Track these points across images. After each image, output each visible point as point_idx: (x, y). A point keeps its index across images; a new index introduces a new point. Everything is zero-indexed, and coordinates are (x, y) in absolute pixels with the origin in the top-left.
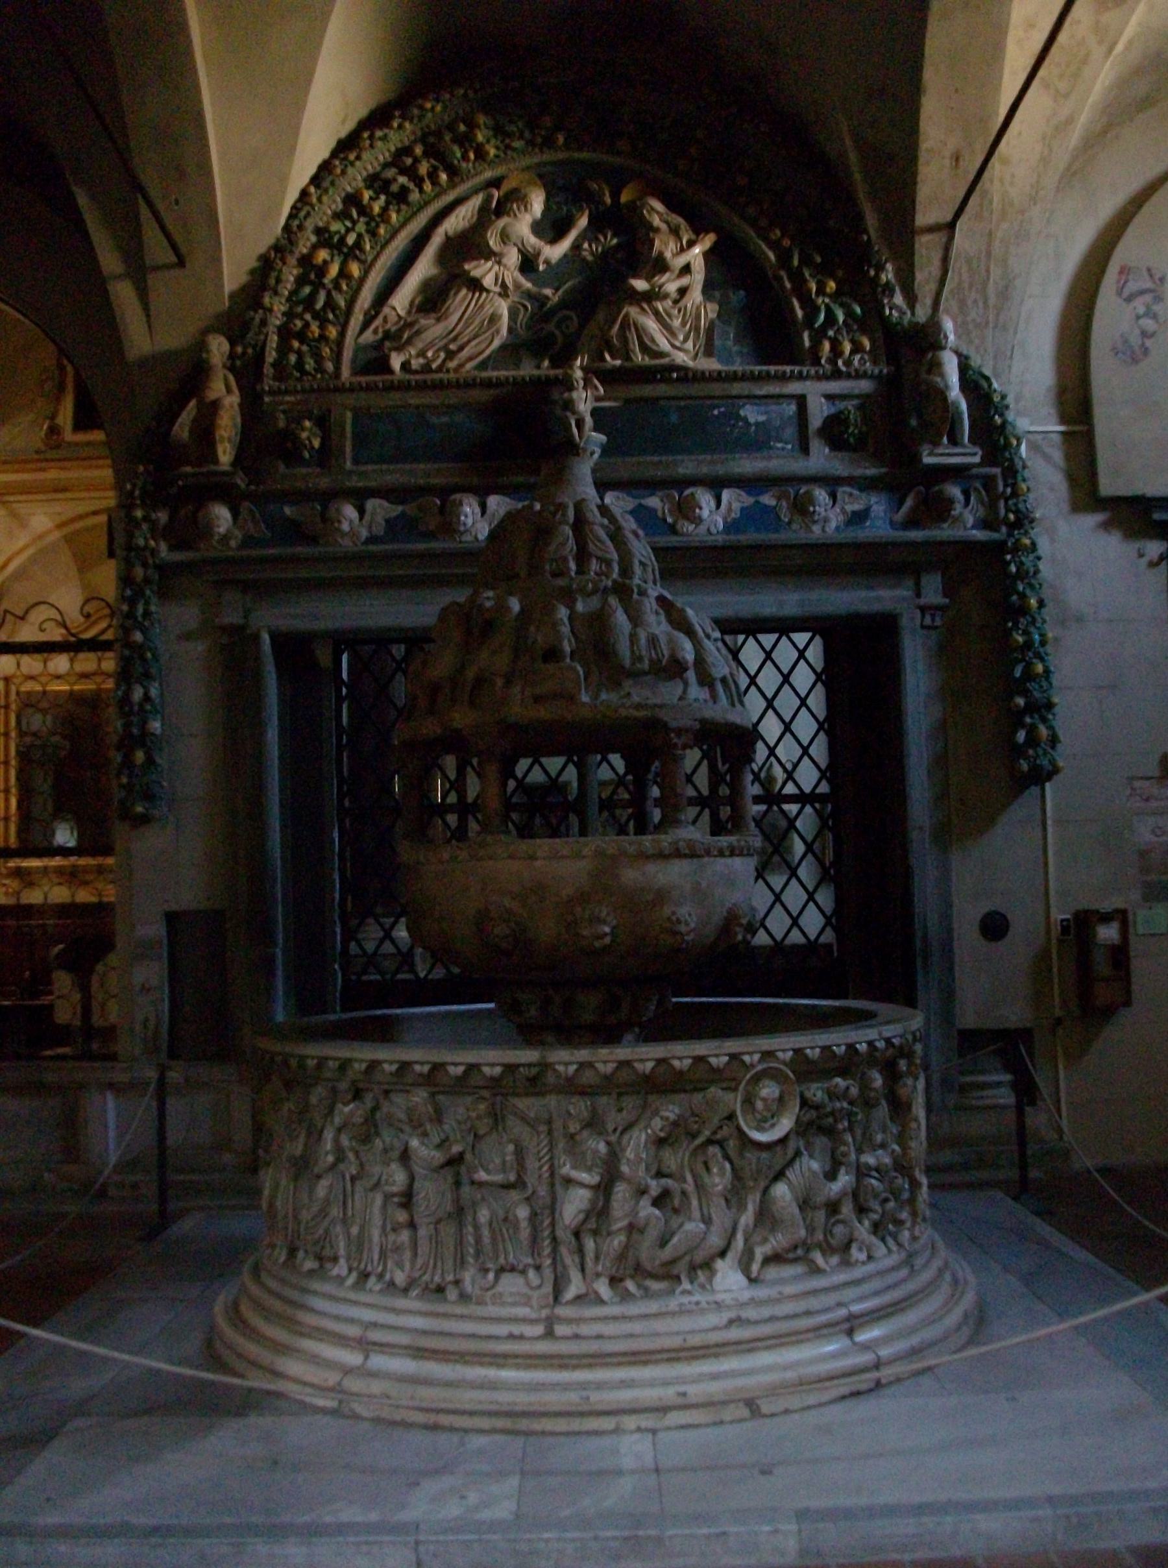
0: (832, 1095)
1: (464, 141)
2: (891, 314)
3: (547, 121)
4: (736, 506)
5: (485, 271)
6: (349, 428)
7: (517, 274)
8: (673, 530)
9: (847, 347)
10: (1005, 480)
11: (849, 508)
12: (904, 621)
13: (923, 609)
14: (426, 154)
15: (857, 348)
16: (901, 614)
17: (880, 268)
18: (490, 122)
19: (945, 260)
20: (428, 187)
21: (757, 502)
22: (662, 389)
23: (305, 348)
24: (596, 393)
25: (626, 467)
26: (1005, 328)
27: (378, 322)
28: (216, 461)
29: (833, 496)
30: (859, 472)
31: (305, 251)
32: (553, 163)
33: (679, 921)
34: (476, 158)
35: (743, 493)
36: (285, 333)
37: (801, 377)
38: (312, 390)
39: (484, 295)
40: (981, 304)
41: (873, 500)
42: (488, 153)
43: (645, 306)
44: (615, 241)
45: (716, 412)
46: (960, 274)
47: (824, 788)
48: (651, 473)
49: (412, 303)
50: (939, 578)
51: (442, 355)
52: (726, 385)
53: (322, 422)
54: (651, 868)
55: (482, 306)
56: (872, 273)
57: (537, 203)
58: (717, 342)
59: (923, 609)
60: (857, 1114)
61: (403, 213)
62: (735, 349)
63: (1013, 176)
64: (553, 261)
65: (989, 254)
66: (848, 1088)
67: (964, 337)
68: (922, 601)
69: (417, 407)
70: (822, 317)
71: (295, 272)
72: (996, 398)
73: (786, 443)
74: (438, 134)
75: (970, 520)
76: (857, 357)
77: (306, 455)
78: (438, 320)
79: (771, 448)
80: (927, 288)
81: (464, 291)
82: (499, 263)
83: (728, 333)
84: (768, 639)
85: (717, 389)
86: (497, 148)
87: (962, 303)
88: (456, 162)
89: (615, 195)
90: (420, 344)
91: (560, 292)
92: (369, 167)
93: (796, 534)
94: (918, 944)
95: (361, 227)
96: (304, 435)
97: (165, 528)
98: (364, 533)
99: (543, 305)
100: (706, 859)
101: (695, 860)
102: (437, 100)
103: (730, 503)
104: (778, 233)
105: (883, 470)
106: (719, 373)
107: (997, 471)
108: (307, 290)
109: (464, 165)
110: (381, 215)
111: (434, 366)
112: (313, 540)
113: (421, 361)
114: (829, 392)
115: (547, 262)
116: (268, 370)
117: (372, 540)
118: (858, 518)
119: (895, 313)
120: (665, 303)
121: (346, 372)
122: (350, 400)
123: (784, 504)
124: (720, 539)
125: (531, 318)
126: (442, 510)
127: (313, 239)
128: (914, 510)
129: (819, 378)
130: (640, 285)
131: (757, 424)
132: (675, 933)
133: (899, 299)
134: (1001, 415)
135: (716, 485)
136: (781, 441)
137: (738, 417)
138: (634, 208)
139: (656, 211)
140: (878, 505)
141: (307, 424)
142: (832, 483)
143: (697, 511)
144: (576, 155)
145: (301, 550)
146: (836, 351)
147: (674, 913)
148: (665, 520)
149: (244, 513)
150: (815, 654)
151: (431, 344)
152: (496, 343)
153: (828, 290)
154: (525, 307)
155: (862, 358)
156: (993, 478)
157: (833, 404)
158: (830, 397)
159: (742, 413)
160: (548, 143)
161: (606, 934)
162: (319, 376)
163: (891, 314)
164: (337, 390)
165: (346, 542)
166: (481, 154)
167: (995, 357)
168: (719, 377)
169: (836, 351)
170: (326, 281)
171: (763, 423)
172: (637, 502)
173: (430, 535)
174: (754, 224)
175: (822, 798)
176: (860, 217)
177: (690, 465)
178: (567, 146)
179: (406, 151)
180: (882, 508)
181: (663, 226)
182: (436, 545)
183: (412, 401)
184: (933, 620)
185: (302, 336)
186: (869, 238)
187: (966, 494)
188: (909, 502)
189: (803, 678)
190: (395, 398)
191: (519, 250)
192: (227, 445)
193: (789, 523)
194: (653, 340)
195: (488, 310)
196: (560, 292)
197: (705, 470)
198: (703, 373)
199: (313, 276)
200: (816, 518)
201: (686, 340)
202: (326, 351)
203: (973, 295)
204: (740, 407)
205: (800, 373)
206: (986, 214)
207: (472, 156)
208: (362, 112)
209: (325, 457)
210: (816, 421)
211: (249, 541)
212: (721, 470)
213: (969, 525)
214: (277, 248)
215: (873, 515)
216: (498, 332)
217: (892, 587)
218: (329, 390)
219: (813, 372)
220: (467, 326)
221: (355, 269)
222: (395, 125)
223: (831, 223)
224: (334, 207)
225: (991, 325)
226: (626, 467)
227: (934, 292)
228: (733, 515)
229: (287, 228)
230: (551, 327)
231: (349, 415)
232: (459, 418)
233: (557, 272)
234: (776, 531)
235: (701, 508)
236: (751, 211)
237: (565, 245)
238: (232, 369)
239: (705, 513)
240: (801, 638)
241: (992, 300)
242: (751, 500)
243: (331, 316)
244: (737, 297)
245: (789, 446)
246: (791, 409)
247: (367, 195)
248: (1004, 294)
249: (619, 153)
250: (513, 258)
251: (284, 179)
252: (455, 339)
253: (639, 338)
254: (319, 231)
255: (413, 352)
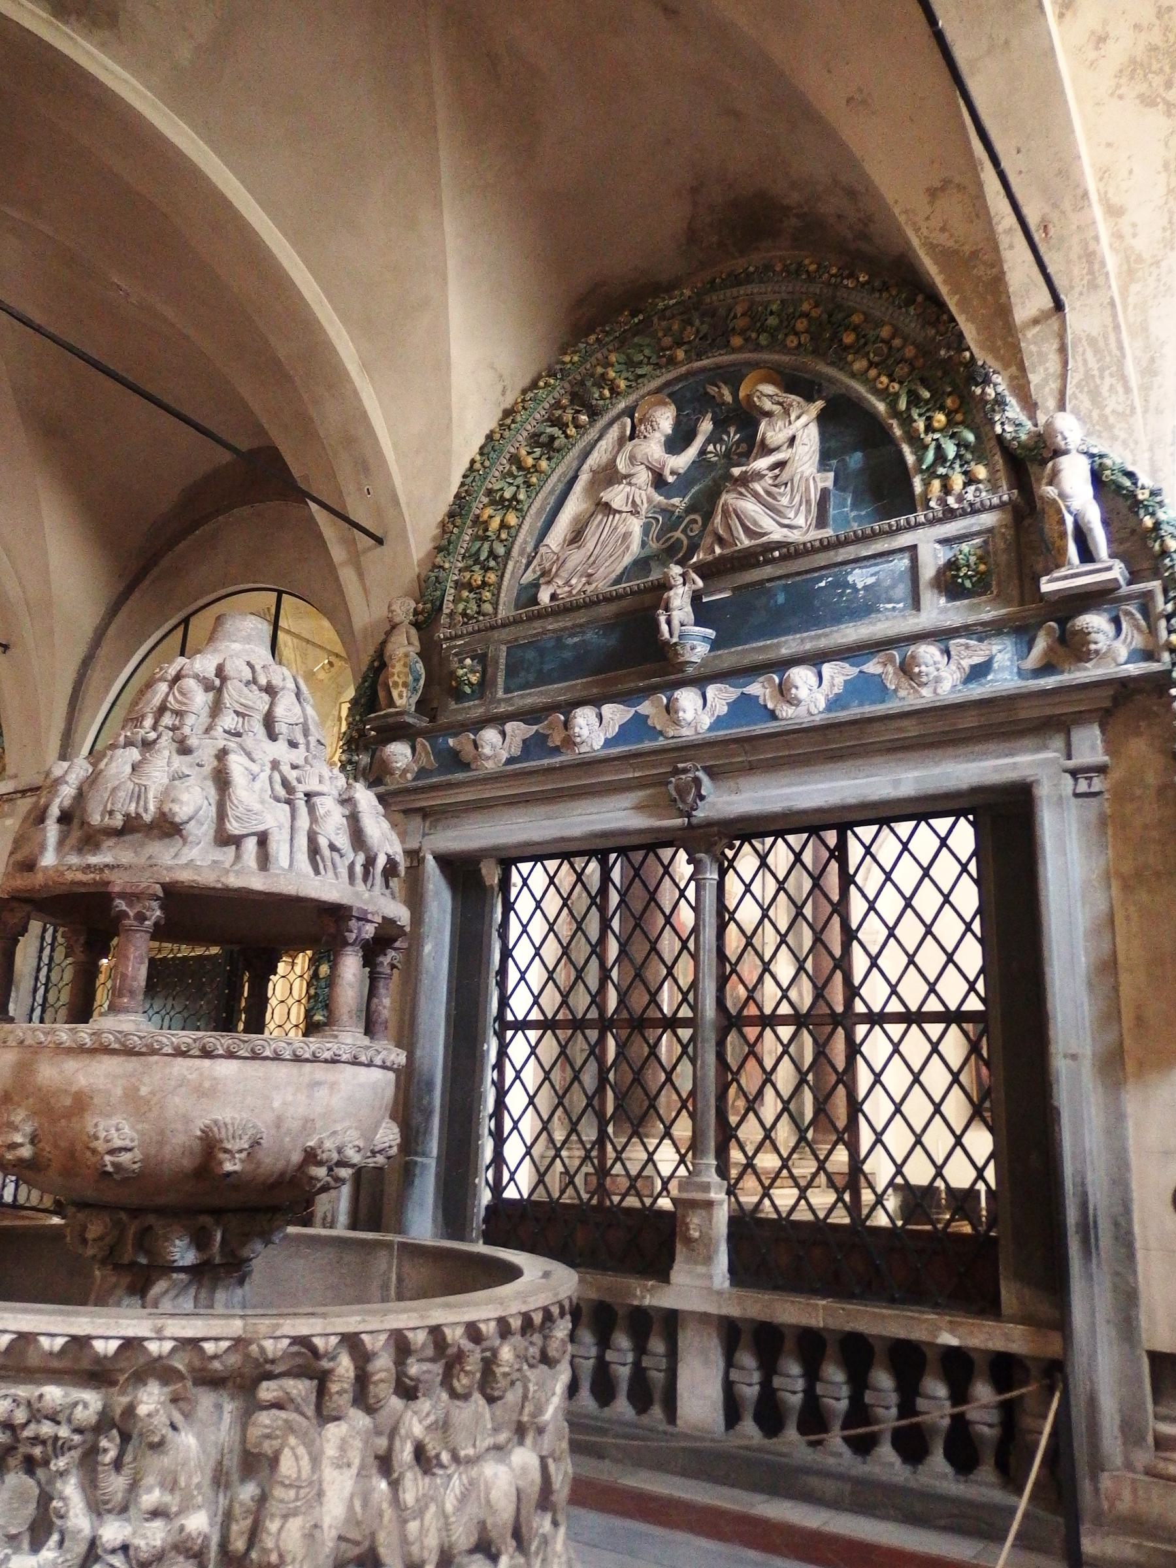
0: (36, 1414)
1: (602, 382)
2: (1004, 430)
3: (667, 341)
4: (840, 680)
5: (616, 496)
6: (502, 661)
7: (651, 490)
8: (773, 716)
9: (957, 481)
10: (1165, 591)
11: (966, 663)
12: (1043, 792)
13: (1074, 773)
14: (572, 402)
15: (970, 480)
16: (1037, 781)
17: (987, 381)
18: (623, 358)
19: (1063, 350)
20: (572, 431)
21: (861, 672)
22: (768, 571)
23: (472, 595)
24: (694, 587)
25: (731, 657)
26: (1159, 411)
27: (535, 562)
28: (391, 703)
29: (947, 652)
30: (971, 619)
31: (478, 512)
32: (678, 379)
33: (97, 1138)
34: (611, 394)
35: (847, 665)
36: (458, 585)
37: (910, 527)
38: (474, 632)
39: (617, 516)
40: (1120, 389)
41: (995, 649)
42: (618, 387)
43: (743, 490)
44: (738, 436)
45: (823, 584)
46: (1085, 361)
47: (974, 1004)
48: (747, 661)
49: (564, 541)
50: (1098, 732)
51: (584, 580)
52: (832, 553)
53: (482, 659)
54: (71, 1065)
55: (616, 528)
56: (978, 391)
57: (665, 420)
58: (832, 512)
59: (1074, 773)
60: (105, 1451)
61: (555, 460)
62: (853, 514)
63: (1134, 225)
64: (681, 471)
65: (1117, 328)
66: (75, 1404)
67: (1105, 434)
68: (1071, 764)
69: (554, 631)
70: (930, 456)
71: (470, 531)
72: (1142, 495)
73: (898, 603)
74: (582, 383)
75: (1123, 653)
76: (971, 489)
77: (468, 690)
78: (579, 548)
79: (878, 611)
80: (1047, 389)
81: (600, 517)
82: (630, 484)
83: (845, 499)
84: (904, 828)
85: (821, 559)
86: (626, 379)
87: (1095, 396)
88: (594, 402)
89: (735, 394)
90: (564, 574)
91: (686, 500)
92: (529, 427)
93: (907, 698)
94: (1072, 1216)
95: (520, 481)
96: (461, 672)
97: (365, 769)
98: (504, 756)
99: (673, 512)
100: (156, 1058)
101: (134, 1058)
102: (574, 352)
103: (832, 677)
104: (884, 379)
105: (1003, 611)
106: (821, 540)
107: (1156, 585)
108: (478, 544)
109: (601, 402)
110: (534, 466)
111: (574, 592)
112: (466, 766)
113: (567, 589)
114: (941, 537)
115: (672, 473)
116: (444, 620)
117: (510, 761)
118: (979, 672)
119: (1008, 428)
120: (762, 482)
121: (503, 613)
122: (505, 634)
123: (890, 669)
124: (818, 719)
125: (661, 529)
126: (566, 725)
127: (486, 500)
128: (1050, 650)
129: (932, 522)
130: (736, 471)
131: (866, 588)
132: (94, 1151)
133: (1014, 410)
134: (1153, 514)
135: (816, 659)
136: (890, 601)
137: (846, 585)
138: (749, 397)
139: (767, 393)
140: (1002, 652)
141: (468, 661)
142: (941, 636)
143: (793, 691)
144: (697, 364)
145: (460, 776)
146: (946, 489)
147: (96, 1125)
148: (765, 706)
149: (418, 747)
150: (964, 837)
151: (572, 574)
152: (627, 560)
153: (936, 425)
154: (657, 520)
155: (977, 489)
156: (1148, 595)
157: (952, 548)
158: (945, 542)
159: (850, 579)
160: (672, 362)
161: (21, 1145)
162: (481, 618)
163: (1004, 430)
164: (492, 628)
165: (490, 765)
166: (615, 391)
167: (1151, 449)
168: (826, 546)
169: (946, 489)
170: (489, 533)
171: (872, 585)
172: (741, 690)
173: (556, 750)
174: (861, 377)
175: (972, 1016)
176: (961, 335)
177: (793, 644)
178: (689, 360)
179: (557, 405)
180: (1007, 656)
181: (777, 408)
182: (556, 760)
183: (550, 627)
184: (1090, 786)
185: (470, 587)
186: (972, 354)
187: (1116, 622)
188: (1041, 644)
189: (945, 870)
190: (537, 626)
191: (648, 468)
192: (401, 688)
193: (896, 691)
194: (755, 523)
195: (622, 530)
196: (686, 500)
197: (808, 646)
198: (804, 544)
199: (480, 532)
200: (924, 679)
201: (796, 514)
202: (487, 595)
203: (1108, 381)
204: (851, 573)
205: (908, 520)
206: (1101, 280)
207: (607, 393)
208: (526, 382)
209: (484, 687)
210: (928, 572)
211: (422, 773)
212: (823, 643)
213: (1122, 659)
214: (451, 515)
215: (996, 666)
216: (628, 548)
217: (1038, 750)
218: (486, 630)
219: (922, 519)
220: (604, 546)
221: (512, 519)
222: (541, 384)
223: (942, 352)
224: (501, 468)
225: (1139, 410)
226: (731, 657)
227: (1056, 393)
228: (836, 691)
229: (457, 496)
230: (678, 534)
231: (504, 648)
232: (590, 635)
233: (686, 480)
234: (883, 701)
235: (797, 688)
236: (859, 365)
237: (692, 452)
238: (416, 624)
239: (802, 693)
240: (942, 824)
241: (1134, 380)
242: (854, 671)
243: (492, 563)
244: (855, 460)
245: (901, 605)
246: (903, 563)
247: (523, 452)
248: (1150, 370)
249: (734, 351)
250: (643, 477)
251: (448, 453)
252: (594, 562)
253: (743, 525)
254: (489, 492)
255: (560, 583)
